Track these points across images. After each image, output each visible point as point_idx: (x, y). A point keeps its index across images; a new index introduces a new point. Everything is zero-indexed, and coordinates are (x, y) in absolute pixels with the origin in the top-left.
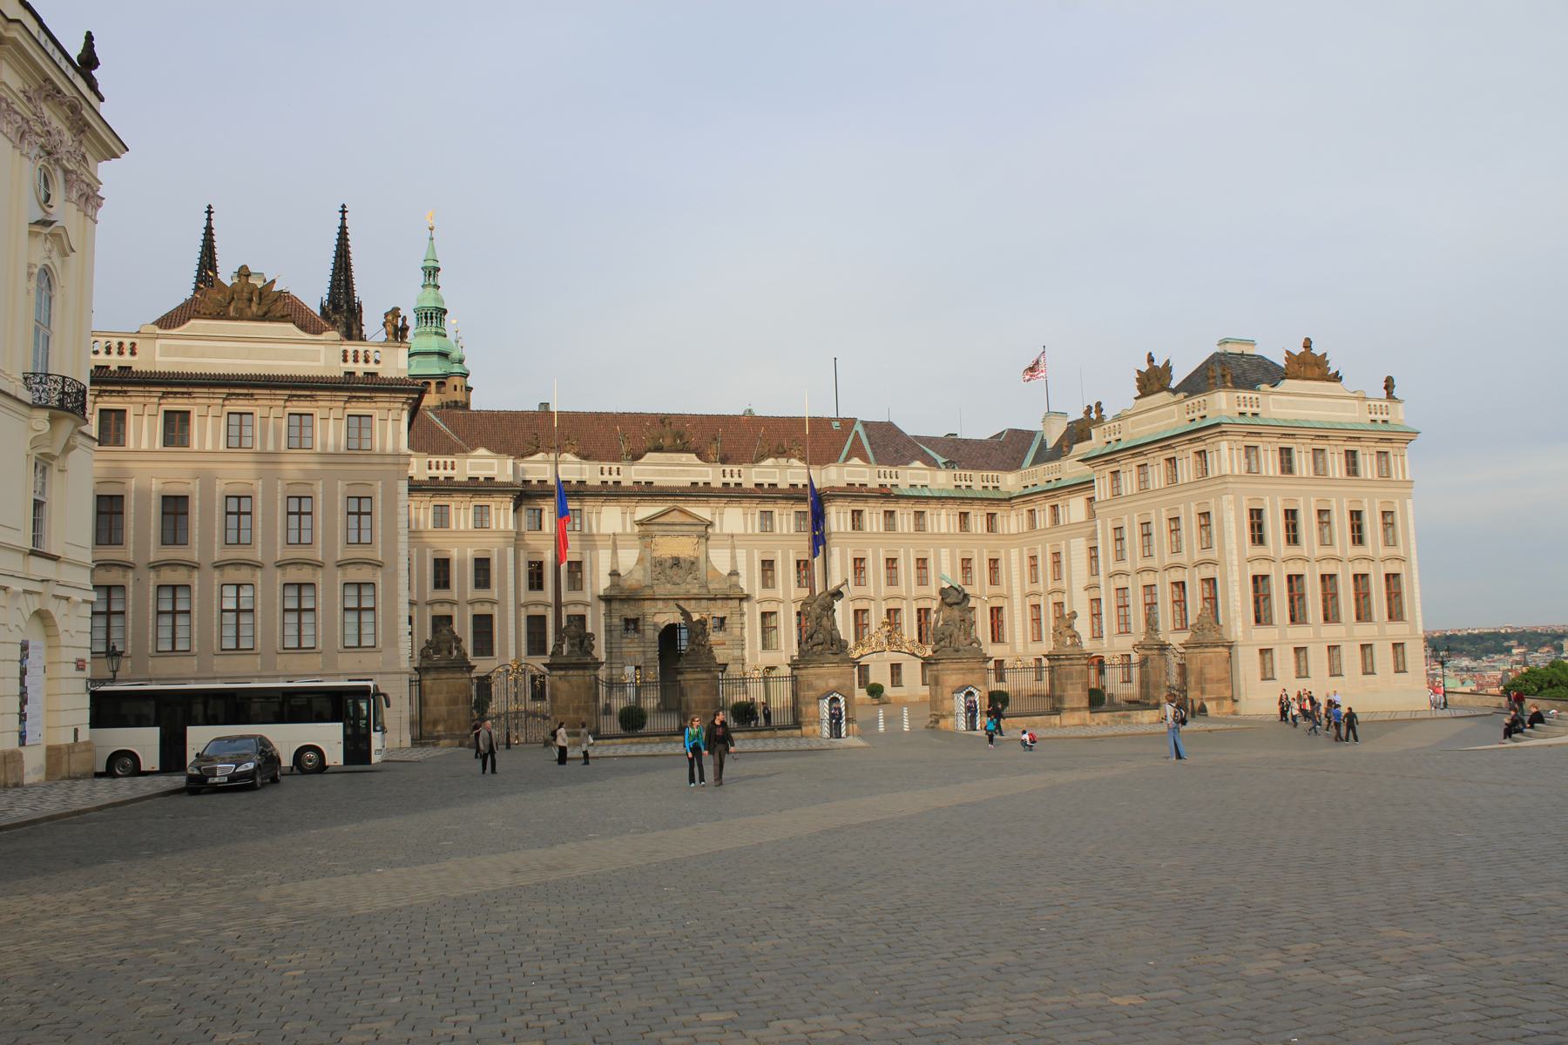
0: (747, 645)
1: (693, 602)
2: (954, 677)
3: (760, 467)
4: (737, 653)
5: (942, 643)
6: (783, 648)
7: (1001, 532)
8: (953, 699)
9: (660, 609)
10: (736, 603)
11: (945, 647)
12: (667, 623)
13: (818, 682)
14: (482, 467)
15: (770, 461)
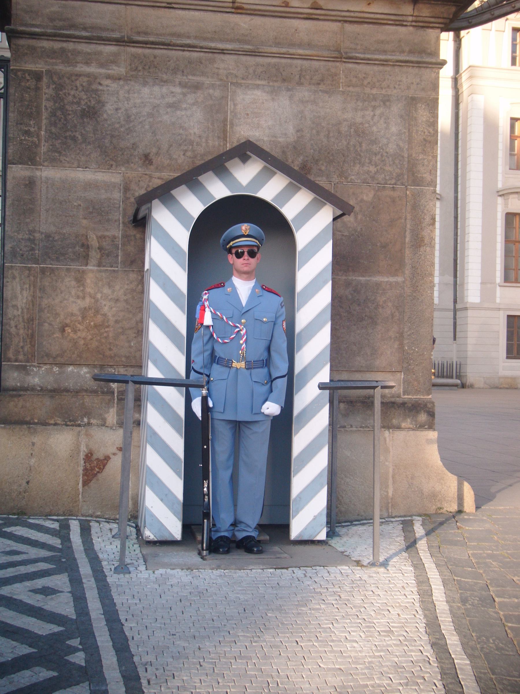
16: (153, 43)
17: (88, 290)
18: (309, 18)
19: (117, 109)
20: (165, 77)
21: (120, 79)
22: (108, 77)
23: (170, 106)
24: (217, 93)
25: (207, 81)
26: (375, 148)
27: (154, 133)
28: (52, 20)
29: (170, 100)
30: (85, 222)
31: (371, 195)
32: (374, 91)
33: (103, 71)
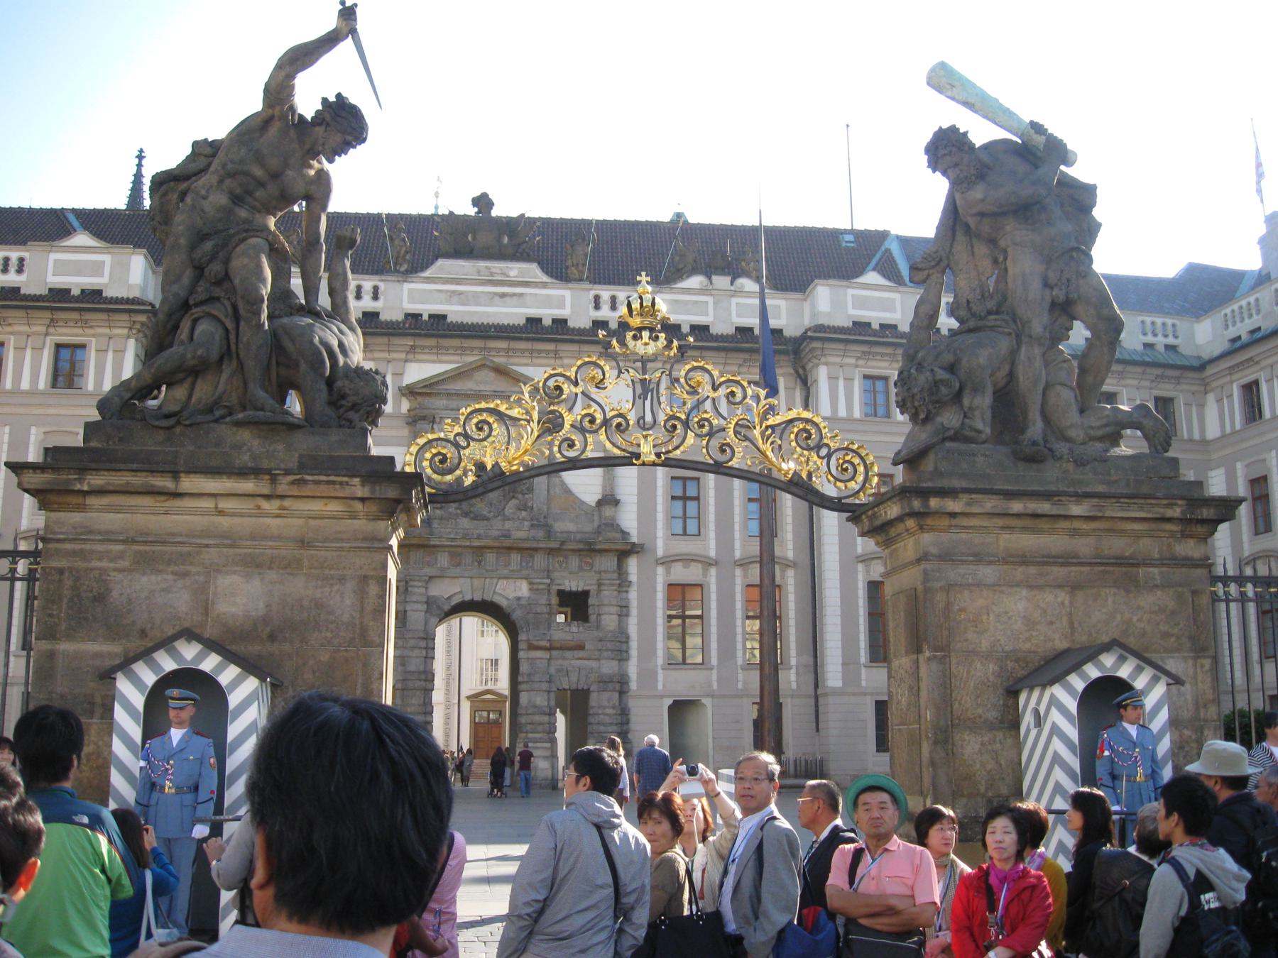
0: (634, 653)
1: (515, 557)
2: (1017, 604)
3: (672, 291)
4: (608, 667)
5: (950, 418)
6: (714, 661)
7: (1186, 436)
8: (1015, 725)
9: (443, 569)
10: (609, 562)
11: (957, 436)
12: (455, 601)
13: (145, 583)
14: (80, 269)
15: (696, 281)
16: (151, 542)
17: (92, 738)
18: (278, 516)
19: (121, 594)
20: (161, 567)
21: (124, 571)
22: (116, 570)
23: (163, 590)
24: (202, 579)
25: (193, 569)
26: (332, 618)
27: (150, 612)
28: (74, 528)
29: (164, 585)
30: (92, 684)
31: (327, 656)
32: (332, 572)
33: (112, 565)
